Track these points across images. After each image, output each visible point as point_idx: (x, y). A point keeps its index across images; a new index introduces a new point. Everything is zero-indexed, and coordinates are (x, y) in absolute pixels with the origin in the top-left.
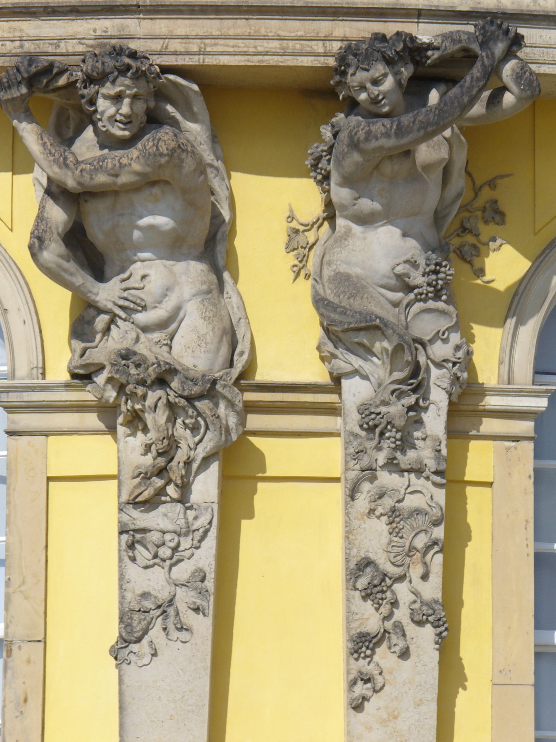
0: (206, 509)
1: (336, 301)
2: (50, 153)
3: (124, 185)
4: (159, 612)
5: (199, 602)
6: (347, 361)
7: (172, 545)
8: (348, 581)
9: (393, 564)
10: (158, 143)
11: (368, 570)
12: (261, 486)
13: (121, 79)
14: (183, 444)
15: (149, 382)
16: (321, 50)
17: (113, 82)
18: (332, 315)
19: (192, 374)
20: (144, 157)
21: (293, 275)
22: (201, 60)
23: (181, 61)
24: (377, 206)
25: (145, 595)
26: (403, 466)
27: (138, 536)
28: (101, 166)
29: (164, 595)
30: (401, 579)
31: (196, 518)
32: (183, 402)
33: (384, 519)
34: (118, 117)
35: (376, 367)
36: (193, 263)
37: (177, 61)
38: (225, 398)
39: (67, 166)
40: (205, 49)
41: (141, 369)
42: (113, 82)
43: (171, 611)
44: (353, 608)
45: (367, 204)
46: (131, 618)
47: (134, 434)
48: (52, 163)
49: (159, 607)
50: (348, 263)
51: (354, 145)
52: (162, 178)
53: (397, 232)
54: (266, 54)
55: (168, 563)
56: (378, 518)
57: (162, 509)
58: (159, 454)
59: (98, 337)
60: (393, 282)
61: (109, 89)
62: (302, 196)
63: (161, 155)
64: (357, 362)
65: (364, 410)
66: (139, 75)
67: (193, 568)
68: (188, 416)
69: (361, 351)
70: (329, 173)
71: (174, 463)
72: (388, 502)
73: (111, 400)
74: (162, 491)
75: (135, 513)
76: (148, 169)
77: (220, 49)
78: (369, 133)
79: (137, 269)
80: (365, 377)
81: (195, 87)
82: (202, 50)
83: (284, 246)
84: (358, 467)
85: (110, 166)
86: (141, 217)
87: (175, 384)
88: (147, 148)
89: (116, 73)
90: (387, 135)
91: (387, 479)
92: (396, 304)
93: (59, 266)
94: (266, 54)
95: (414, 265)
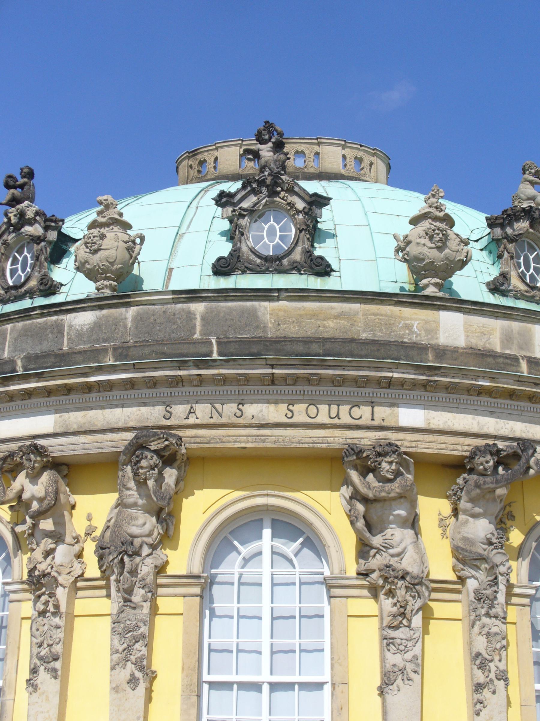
0: (418, 630)
1: (464, 547)
3: (392, 497)
4: (400, 672)
5: (416, 669)
6: (468, 571)
7: (405, 645)
8: (471, 661)
9: (488, 655)
11: (480, 657)
12: (431, 621)
13: (393, 455)
14: (410, 603)
15: (400, 577)
16: (460, 449)
17: (390, 456)
18: (465, 553)
19: (413, 575)
21: (441, 537)
24: (481, 511)
25: (394, 665)
26: (492, 615)
27: (391, 641)
29: (401, 665)
30: (491, 661)
31: (414, 634)
32: (412, 586)
33: (485, 636)
34: (390, 470)
35: (482, 575)
36: (410, 530)
38: (425, 585)
39: (370, 489)
41: (395, 572)
42: (390, 456)
43: (405, 672)
44: (474, 673)
45: (477, 510)
46: (390, 675)
47: (388, 599)
49: (400, 670)
50: (468, 533)
51: (477, 486)
53: (487, 521)
54: (440, 449)
55: (403, 652)
56: (482, 636)
57: (401, 629)
58: (401, 607)
59: (370, 558)
60: (485, 541)
61: (388, 459)
62: (444, 506)
63: (408, 486)
64: (473, 572)
65: (476, 592)
66: (400, 455)
67: (413, 655)
68: (412, 592)
69: (475, 568)
70: (461, 497)
71: (407, 611)
72: (486, 629)
73: (381, 584)
74: (401, 622)
75: (390, 631)
76: (402, 492)
77: (423, 446)
78: (485, 482)
79: (389, 532)
80: (476, 579)
81: (412, 460)
83: (437, 525)
84: (474, 615)
85: (387, 489)
86: (395, 511)
87: (408, 579)
90: (492, 483)
91: (485, 620)
92: (485, 550)
93: (363, 529)
94: (440, 449)
95: (493, 535)
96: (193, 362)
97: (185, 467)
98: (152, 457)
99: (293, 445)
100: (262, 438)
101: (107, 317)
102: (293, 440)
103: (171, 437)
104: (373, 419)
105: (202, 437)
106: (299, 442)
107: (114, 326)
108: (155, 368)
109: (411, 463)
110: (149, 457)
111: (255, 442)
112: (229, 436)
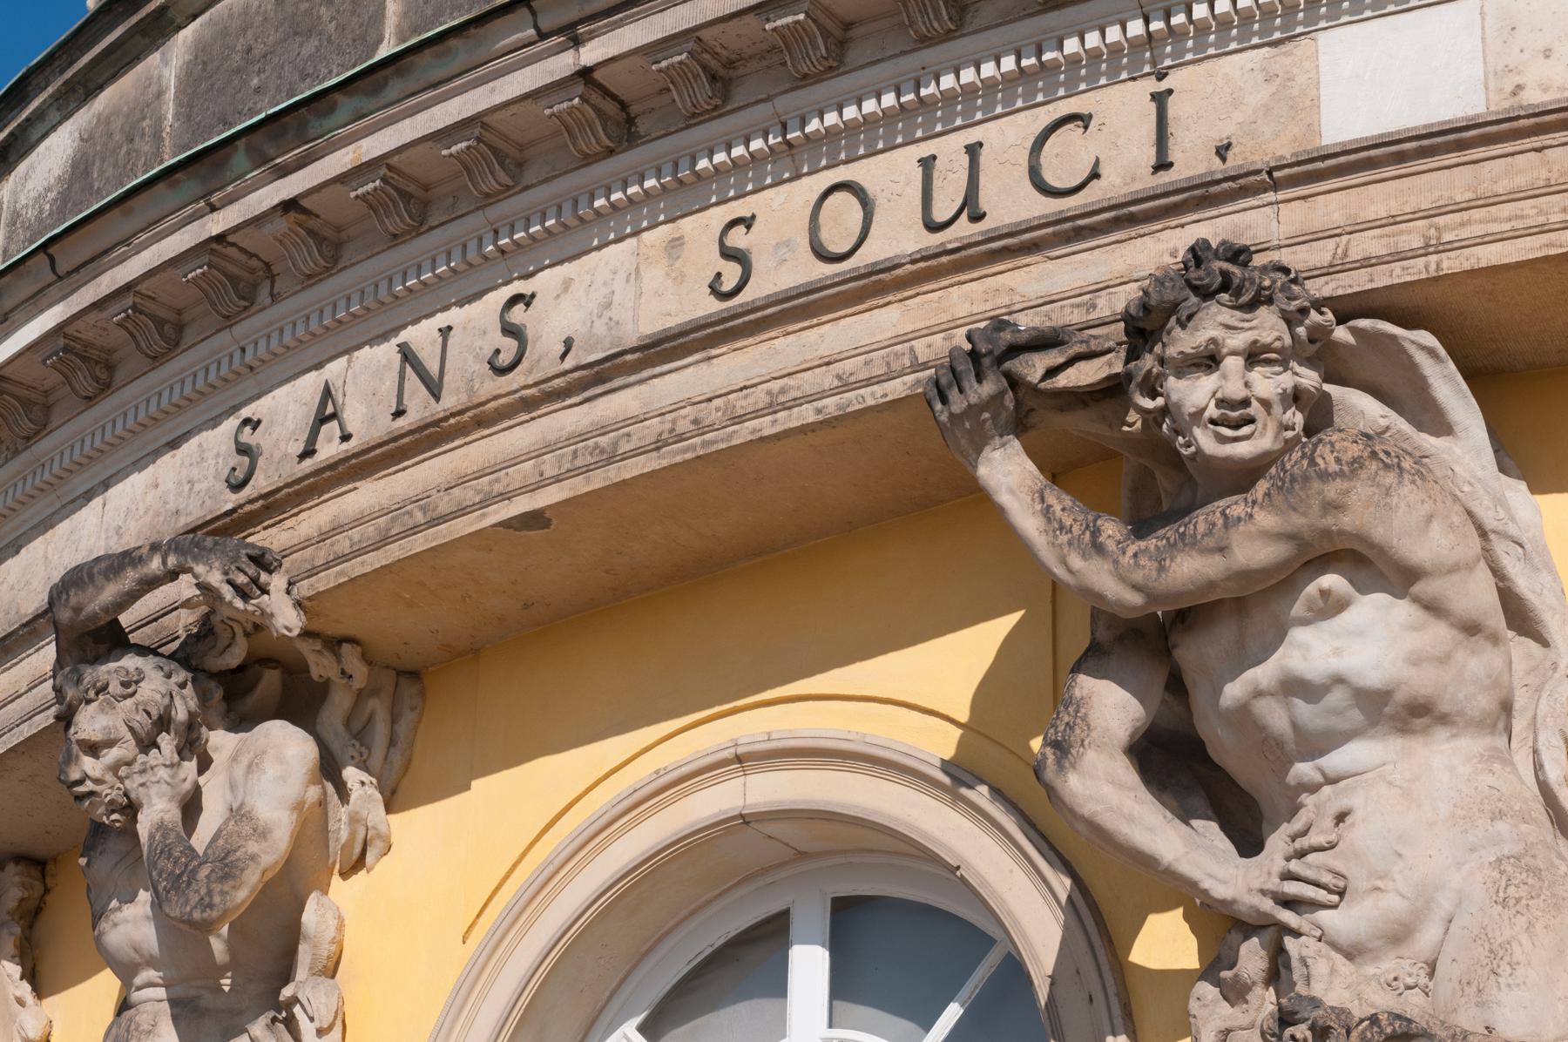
2: (1061, 528)
10: (1314, 451)
20: (1281, 488)
22: (1433, 267)
23: (1382, 278)
28: (1184, 534)
37: (1372, 281)
39: (1099, 549)
40: (1439, 238)
48: (1066, 550)
52: (1340, 547)
61: (1184, 341)
63: (1325, 476)
81: (1427, 338)
82: (1433, 242)
88: (1288, 466)
89: (1194, 299)
96: (250, 150)
97: (394, 720)
98: (130, 684)
99: (744, 433)
100: (603, 441)
101: (108, 121)
102: (742, 403)
103: (196, 559)
104: (1162, 165)
105: (359, 521)
106: (772, 408)
107: (124, 149)
108: (125, 241)
109: (1421, 358)
110: (115, 687)
111: (573, 473)
112: (462, 481)
